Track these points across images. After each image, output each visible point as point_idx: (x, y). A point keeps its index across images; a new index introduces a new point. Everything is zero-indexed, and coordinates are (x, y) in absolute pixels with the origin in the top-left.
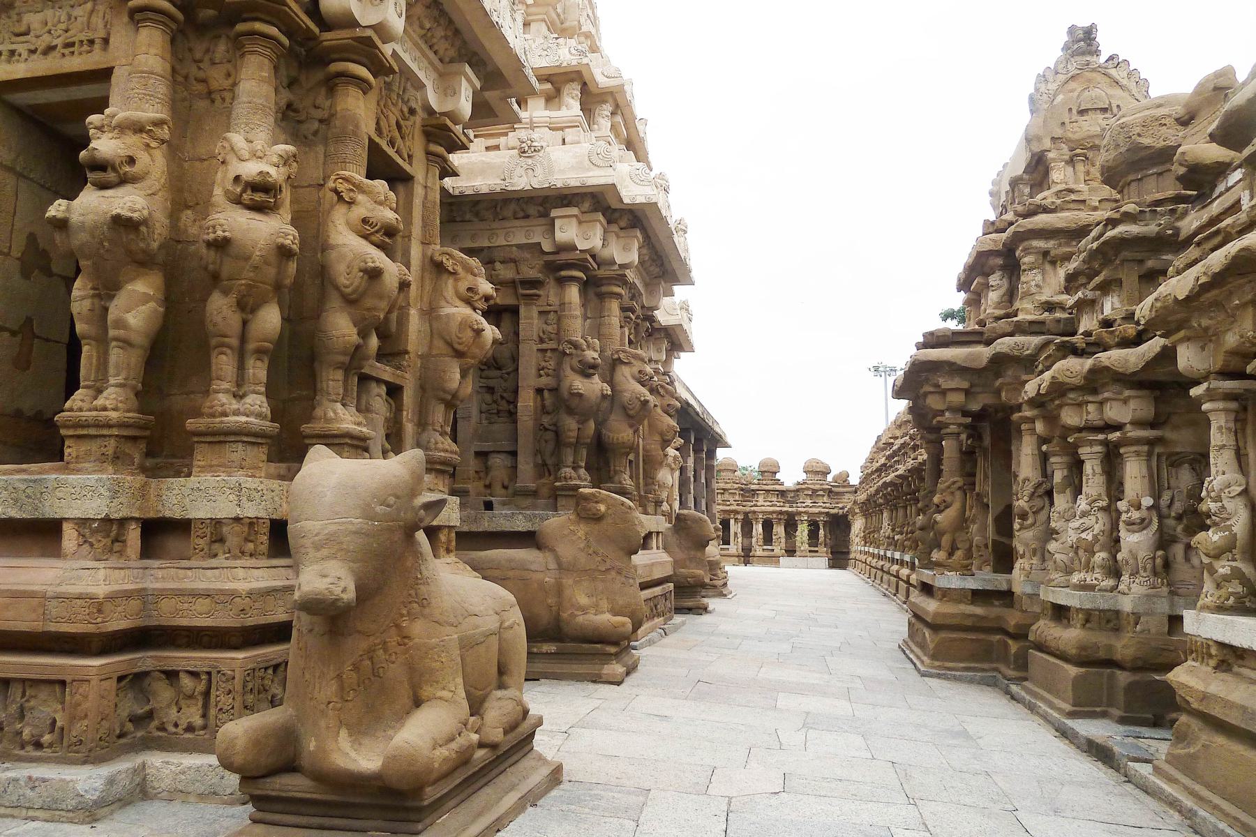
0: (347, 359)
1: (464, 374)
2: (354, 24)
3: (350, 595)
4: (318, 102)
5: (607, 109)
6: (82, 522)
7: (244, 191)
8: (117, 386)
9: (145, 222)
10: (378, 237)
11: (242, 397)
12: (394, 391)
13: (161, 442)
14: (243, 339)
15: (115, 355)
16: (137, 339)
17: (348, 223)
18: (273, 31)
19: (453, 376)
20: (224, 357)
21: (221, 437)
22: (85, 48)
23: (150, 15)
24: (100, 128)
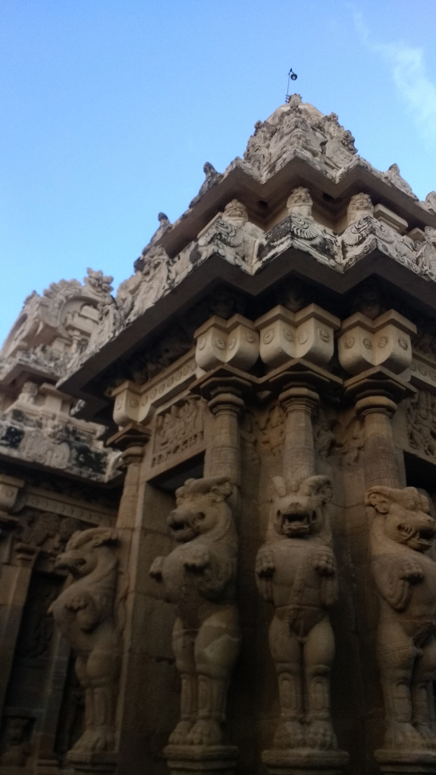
0: (408, 674)
2: (369, 366)
4: (355, 434)
7: (283, 522)
8: (205, 718)
9: (207, 565)
10: (415, 541)
11: (309, 724)
14: (302, 661)
15: (203, 686)
17: (386, 533)
18: (304, 391)
20: (286, 683)
22: (193, 441)
23: (221, 407)
24: (182, 496)
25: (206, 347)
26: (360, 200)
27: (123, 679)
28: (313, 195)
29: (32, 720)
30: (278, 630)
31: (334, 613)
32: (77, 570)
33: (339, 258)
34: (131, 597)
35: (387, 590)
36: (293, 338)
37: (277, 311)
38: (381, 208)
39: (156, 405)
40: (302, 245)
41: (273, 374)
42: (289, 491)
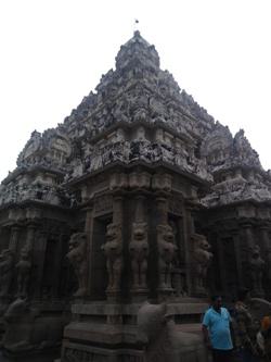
1: (203, 267)
3: (146, 339)
5: (252, 173)
12: (183, 275)
13: (125, 296)
15: (115, 277)
19: (200, 269)
21: (137, 294)
25: (113, 183)
30: (134, 264)
32: (75, 245)
36: (138, 182)
42: (138, 227)
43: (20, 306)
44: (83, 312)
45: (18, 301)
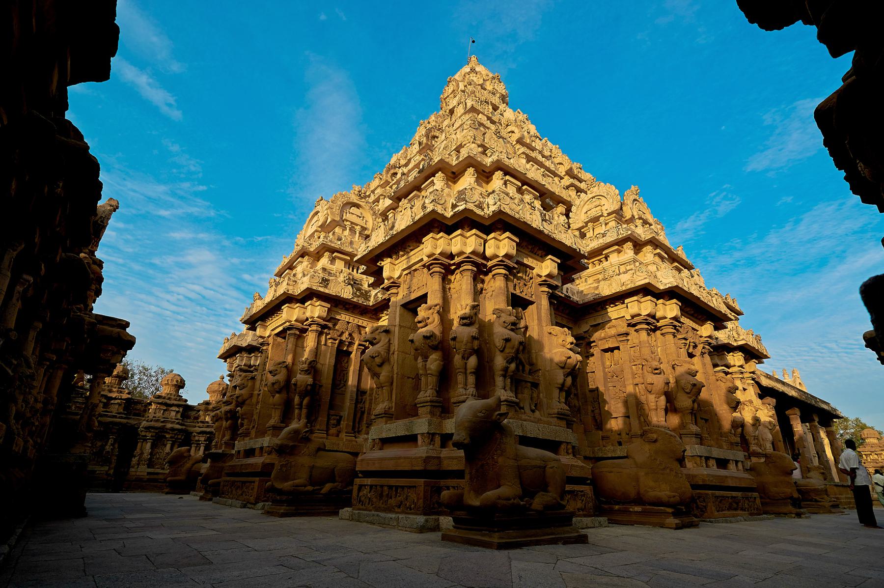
6: (423, 434)
9: (431, 336)
14: (466, 369)
16: (434, 373)
26: (498, 174)
27: (395, 384)
28: (476, 171)
29: (341, 417)
30: (457, 359)
31: (478, 352)
33: (486, 210)
34: (396, 353)
35: (498, 344)
37: (459, 232)
38: (508, 177)
39: (404, 270)
40: (471, 206)
41: (457, 260)
43: (296, 432)
44: (384, 435)
45: (294, 425)
